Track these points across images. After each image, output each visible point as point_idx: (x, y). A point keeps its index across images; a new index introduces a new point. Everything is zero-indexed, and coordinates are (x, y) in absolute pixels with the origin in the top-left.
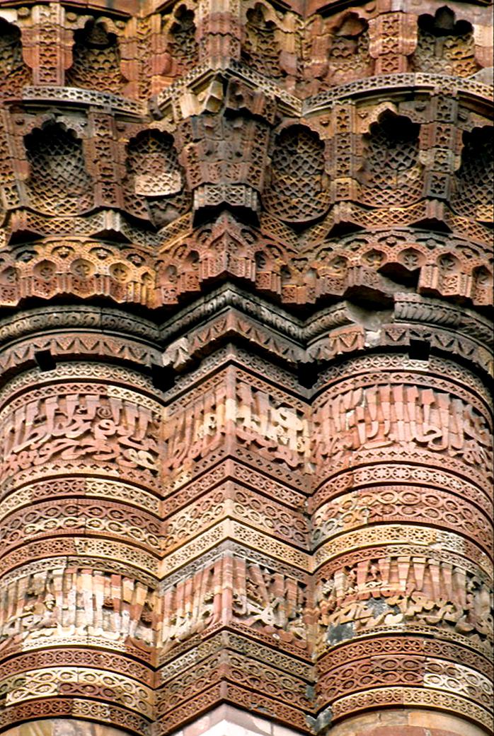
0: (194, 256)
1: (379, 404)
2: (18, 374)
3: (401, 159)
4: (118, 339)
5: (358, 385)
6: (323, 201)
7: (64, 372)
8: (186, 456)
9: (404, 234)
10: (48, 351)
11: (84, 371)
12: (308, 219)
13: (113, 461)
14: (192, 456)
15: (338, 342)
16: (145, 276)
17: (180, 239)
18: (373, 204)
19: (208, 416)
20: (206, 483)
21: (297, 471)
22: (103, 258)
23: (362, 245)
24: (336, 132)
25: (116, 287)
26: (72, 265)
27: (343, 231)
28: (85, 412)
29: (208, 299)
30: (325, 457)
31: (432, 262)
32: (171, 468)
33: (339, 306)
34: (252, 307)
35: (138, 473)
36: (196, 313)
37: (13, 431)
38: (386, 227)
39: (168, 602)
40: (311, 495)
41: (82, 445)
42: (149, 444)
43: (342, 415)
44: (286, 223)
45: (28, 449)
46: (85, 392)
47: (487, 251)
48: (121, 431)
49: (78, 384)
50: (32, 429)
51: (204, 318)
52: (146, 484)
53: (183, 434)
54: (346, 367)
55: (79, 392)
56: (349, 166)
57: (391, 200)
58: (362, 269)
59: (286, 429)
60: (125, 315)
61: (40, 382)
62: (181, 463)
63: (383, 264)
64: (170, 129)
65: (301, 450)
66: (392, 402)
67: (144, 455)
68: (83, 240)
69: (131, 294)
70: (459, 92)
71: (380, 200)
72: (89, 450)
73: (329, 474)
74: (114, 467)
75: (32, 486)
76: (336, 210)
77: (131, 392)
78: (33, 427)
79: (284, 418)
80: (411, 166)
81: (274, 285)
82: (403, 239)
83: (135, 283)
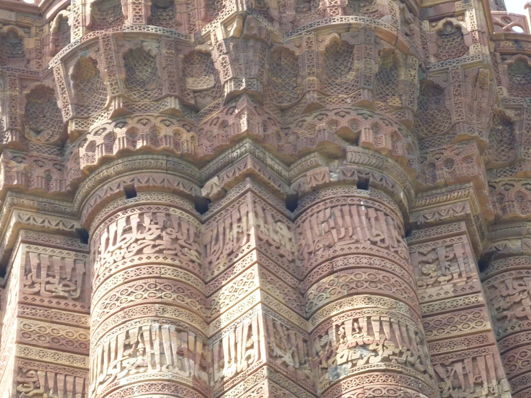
0: (224, 124)
1: (343, 217)
2: (112, 200)
3: (342, 68)
4: (176, 177)
5: (327, 205)
6: (298, 92)
7: (142, 198)
8: (222, 253)
9: (349, 110)
10: (133, 186)
11: (155, 198)
12: (289, 104)
13: (176, 255)
14: (225, 253)
15: (313, 178)
16: (192, 137)
17: (214, 115)
18: (328, 93)
19: (235, 226)
21: (292, 264)
22: (168, 126)
23: (325, 116)
24: (306, 50)
26: (150, 129)
28: (156, 223)
30: (310, 253)
31: (367, 126)
33: (312, 155)
34: (261, 155)
35: (191, 264)
36: (227, 159)
37: (108, 239)
38: (338, 106)
40: (303, 281)
41: (156, 244)
42: (195, 246)
43: (320, 226)
44: (276, 106)
45: (120, 248)
46: (156, 211)
47: (396, 123)
48: (180, 236)
49: (152, 206)
50: (123, 234)
52: (196, 271)
54: (318, 195)
55: (152, 211)
57: (339, 91)
58: (326, 131)
59: (283, 236)
60: (181, 162)
61: (127, 205)
62: (218, 259)
63: (339, 128)
65: (293, 251)
66: (351, 216)
68: (156, 115)
69: (186, 147)
70: (375, 27)
71: (332, 91)
72: (161, 247)
73: (314, 265)
74: (177, 259)
75: (124, 271)
76: (308, 96)
77: (184, 213)
79: (281, 229)
80: (349, 71)
82: (348, 113)
83: (187, 141)
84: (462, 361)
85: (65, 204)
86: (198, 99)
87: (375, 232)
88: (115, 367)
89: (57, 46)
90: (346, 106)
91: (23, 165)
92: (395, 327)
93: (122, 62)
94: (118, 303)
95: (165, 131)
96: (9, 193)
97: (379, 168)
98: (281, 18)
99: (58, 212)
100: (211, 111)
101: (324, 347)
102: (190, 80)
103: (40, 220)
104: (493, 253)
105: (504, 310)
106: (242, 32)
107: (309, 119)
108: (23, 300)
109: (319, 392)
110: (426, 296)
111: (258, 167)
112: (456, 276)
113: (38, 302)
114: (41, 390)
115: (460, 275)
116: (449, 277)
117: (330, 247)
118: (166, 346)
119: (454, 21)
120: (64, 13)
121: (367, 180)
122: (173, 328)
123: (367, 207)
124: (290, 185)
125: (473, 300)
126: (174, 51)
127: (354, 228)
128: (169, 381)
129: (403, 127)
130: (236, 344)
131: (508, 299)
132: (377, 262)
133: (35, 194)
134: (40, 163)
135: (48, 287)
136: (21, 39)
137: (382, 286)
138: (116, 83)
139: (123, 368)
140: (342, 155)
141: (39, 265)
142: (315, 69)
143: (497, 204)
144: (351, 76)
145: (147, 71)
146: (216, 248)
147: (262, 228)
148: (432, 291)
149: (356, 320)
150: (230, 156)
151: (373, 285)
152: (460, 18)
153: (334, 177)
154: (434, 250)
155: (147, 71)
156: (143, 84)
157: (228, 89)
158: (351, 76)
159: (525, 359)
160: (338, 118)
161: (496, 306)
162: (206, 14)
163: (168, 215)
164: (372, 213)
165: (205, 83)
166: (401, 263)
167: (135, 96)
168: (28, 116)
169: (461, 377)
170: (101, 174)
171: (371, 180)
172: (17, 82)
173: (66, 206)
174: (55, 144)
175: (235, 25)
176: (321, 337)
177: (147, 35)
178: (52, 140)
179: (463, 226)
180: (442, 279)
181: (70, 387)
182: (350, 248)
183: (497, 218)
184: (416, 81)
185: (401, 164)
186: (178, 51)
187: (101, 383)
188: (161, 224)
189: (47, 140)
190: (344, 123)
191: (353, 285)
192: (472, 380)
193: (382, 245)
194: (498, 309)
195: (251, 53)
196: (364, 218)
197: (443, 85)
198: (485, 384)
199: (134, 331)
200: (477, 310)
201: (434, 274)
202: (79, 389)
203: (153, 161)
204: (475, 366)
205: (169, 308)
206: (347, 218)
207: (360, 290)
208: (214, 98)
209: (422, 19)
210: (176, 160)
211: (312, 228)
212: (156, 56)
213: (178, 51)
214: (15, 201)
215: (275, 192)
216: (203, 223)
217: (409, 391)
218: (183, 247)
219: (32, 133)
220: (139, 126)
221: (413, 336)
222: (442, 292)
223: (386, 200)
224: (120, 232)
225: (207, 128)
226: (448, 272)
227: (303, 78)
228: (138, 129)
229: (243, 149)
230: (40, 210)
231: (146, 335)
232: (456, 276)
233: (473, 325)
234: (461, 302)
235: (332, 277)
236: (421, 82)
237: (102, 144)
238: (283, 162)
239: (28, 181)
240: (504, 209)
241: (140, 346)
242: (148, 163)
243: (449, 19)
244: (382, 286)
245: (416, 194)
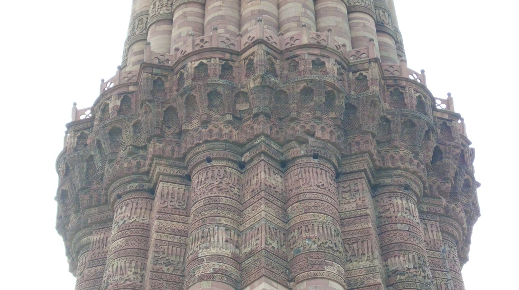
0: (252, 128)
7: (214, 163)
16: (238, 133)
17: (248, 122)
20: (256, 199)
25: (230, 137)
27: (293, 119)
32: (244, 194)
34: (269, 143)
36: (253, 145)
37: (198, 182)
39: (244, 240)
42: (238, 186)
48: (230, 182)
51: (255, 146)
53: (248, 183)
64: (247, 91)
67: (236, 190)
69: (234, 139)
76: (292, 114)
78: (204, 181)
81: (275, 136)
84: (357, 242)
86: (242, 115)
87: (319, 181)
88: (197, 247)
89: (179, 86)
90: (309, 118)
91: (161, 145)
92: (325, 229)
93: (207, 97)
94: (200, 215)
96: (155, 158)
97: (324, 148)
98: (281, 74)
99: (177, 166)
100: (247, 120)
101: (292, 238)
103: (169, 171)
104: (378, 184)
105: (382, 213)
106: (261, 83)
107: (292, 125)
108: (159, 211)
109: (289, 260)
110: (344, 209)
111: (267, 149)
112: (358, 199)
113: (166, 211)
114: (165, 255)
115: (360, 199)
116: (355, 200)
117: (298, 188)
118: (220, 238)
119: (364, 73)
120: (182, 70)
121: (318, 154)
122: (224, 229)
123: (317, 168)
124: (283, 155)
125: (364, 212)
127: (310, 179)
128: (220, 255)
129: (336, 127)
130: (252, 237)
131: (383, 208)
132: (319, 196)
133: (167, 158)
134: (170, 143)
135: (172, 204)
136: (163, 82)
137: (320, 209)
139: (200, 248)
140: (306, 142)
141: (168, 192)
142: (295, 101)
143: (381, 161)
144: (312, 103)
146: (247, 187)
147: (268, 179)
148: (346, 206)
149: (307, 226)
151: (316, 208)
152: (367, 71)
153: (302, 153)
154: (349, 185)
156: (216, 107)
157: (255, 111)
158: (312, 103)
159: (389, 238)
160: (305, 125)
161: (378, 211)
162: (247, 73)
163: (225, 171)
164: (319, 171)
165: (244, 107)
166: (331, 196)
167: (212, 113)
168: (164, 121)
169: (356, 251)
171: (320, 154)
172: (160, 105)
173: (181, 164)
174: (177, 134)
176: (291, 233)
177: (218, 84)
179: (363, 174)
180: (351, 201)
181: (178, 253)
182: (307, 189)
183: (381, 167)
184: (343, 105)
185: (334, 146)
186: (233, 91)
187: (191, 254)
188: (222, 176)
190: (308, 127)
191: (307, 208)
192: (360, 252)
193: (323, 187)
194: (379, 212)
196: (315, 174)
197: (356, 105)
198: (366, 255)
199: (206, 230)
200: (365, 217)
201: (348, 198)
202: (183, 254)
204: (363, 245)
205: (223, 219)
206: (307, 174)
207: (310, 211)
209: (349, 72)
210: (230, 144)
211: (291, 178)
213: (233, 91)
214: (158, 162)
215: (275, 160)
216: (242, 173)
217: (329, 261)
218: (231, 187)
219: (167, 129)
220: (214, 129)
221: (333, 233)
222: (351, 207)
223: (326, 164)
224: (203, 179)
225: (245, 128)
226: (354, 197)
227: (290, 105)
229: (260, 140)
230: (169, 166)
231: (211, 232)
232: (358, 199)
233: (363, 224)
234: (359, 213)
235: (298, 204)
236: (346, 105)
238: (279, 145)
239: (164, 152)
240: (384, 164)
241: (209, 238)
243: (362, 72)
244: (320, 209)
245: (342, 158)
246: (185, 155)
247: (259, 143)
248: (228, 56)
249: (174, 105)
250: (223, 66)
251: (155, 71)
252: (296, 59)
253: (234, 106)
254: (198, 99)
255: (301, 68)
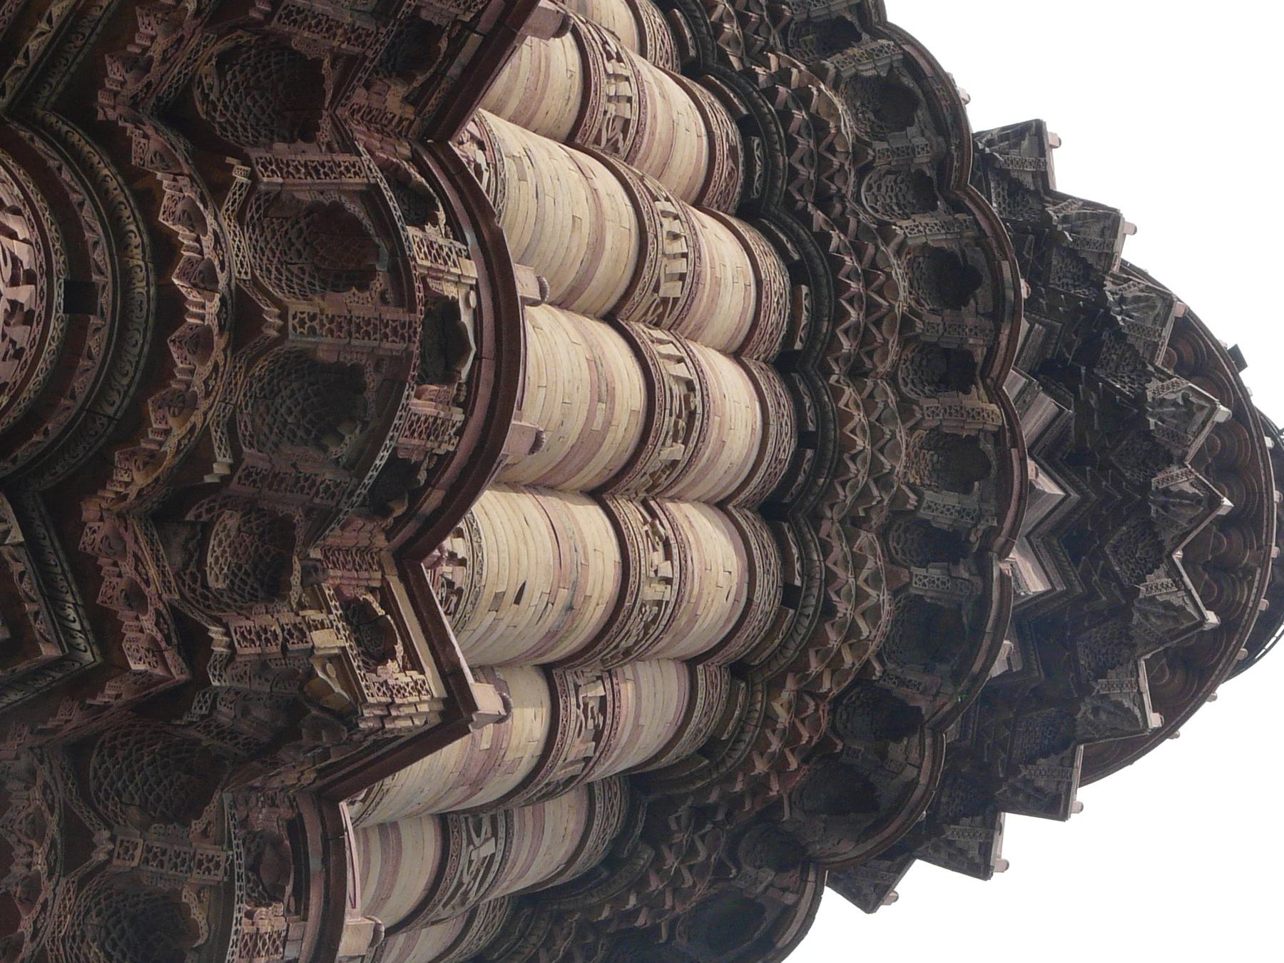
0: (136, 598)
29: (80, 610)
56: (153, 867)
85: (60, 88)
86: (184, 534)
93: (348, 359)
95: (178, 432)
100: (157, 560)
102: (231, 520)
107: (53, 829)
120: (441, 215)
126: (317, 501)
136: (408, 78)
138: (312, 331)
145: (290, 412)
150: (69, 598)
155: (290, 412)
157: (215, 632)
170: (133, 227)
175: (337, 689)
178: (197, 93)
186: (308, 512)
189: (200, 82)
190: (26, 926)
195: (260, 713)
203: (125, 381)
208: (177, 575)
212: (325, 449)
227: (144, 827)
228: (203, 362)
229: (81, 640)
237: (201, 253)
242: (128, 367)
246: (113, 142)
247: (69, 633)
248: (434, 499)
249: (326, 131)
250: (417, 466)
251: (474, 40)
252: (289, 889)
253: (250, 508)
254: (360, 304)
255: (270, 920)
